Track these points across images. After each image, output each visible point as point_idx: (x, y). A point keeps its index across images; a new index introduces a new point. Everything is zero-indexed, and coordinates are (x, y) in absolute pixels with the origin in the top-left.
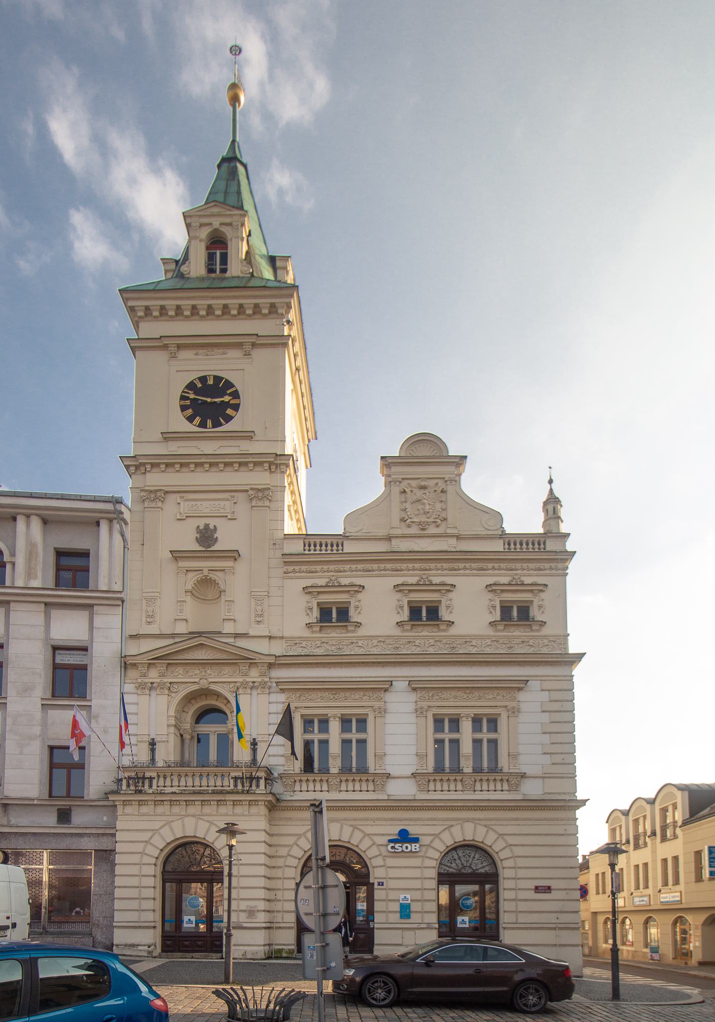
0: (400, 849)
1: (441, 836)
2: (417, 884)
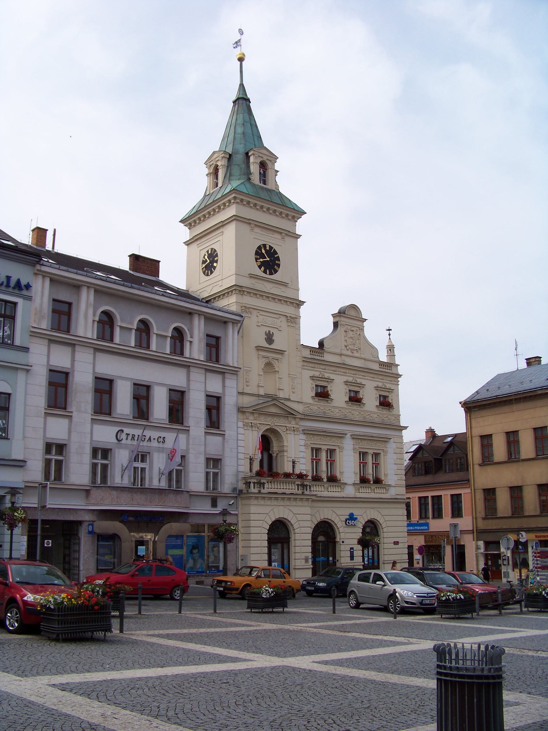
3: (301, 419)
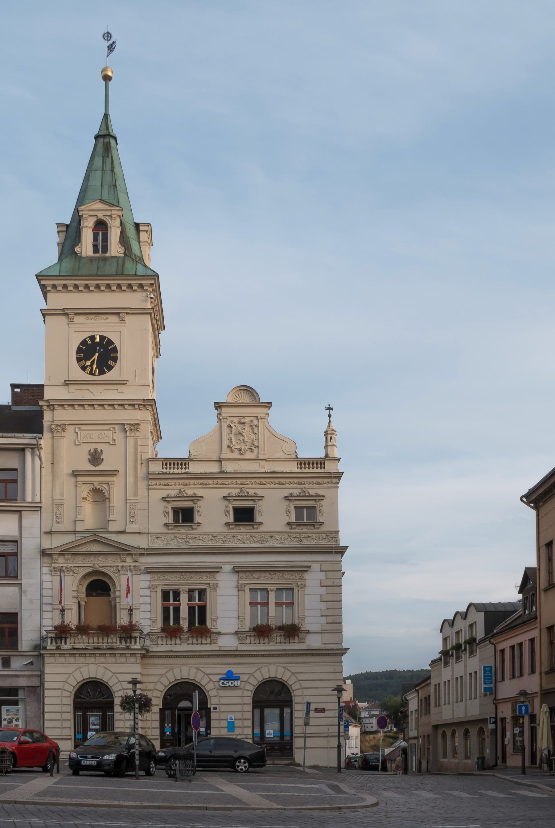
0: (227, 685)
1: (255, 675)
2: (239, 708)
3: (141, 554)
